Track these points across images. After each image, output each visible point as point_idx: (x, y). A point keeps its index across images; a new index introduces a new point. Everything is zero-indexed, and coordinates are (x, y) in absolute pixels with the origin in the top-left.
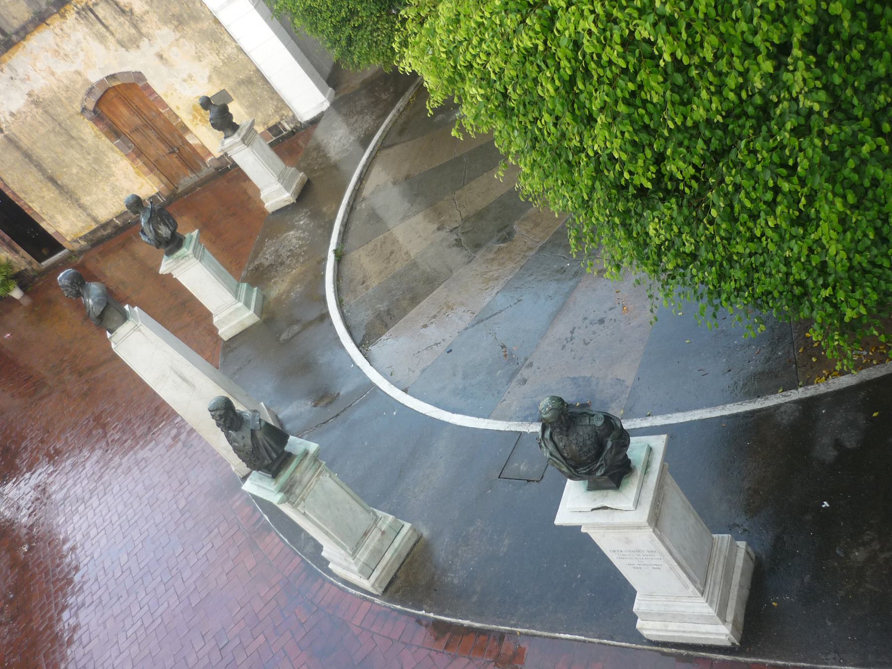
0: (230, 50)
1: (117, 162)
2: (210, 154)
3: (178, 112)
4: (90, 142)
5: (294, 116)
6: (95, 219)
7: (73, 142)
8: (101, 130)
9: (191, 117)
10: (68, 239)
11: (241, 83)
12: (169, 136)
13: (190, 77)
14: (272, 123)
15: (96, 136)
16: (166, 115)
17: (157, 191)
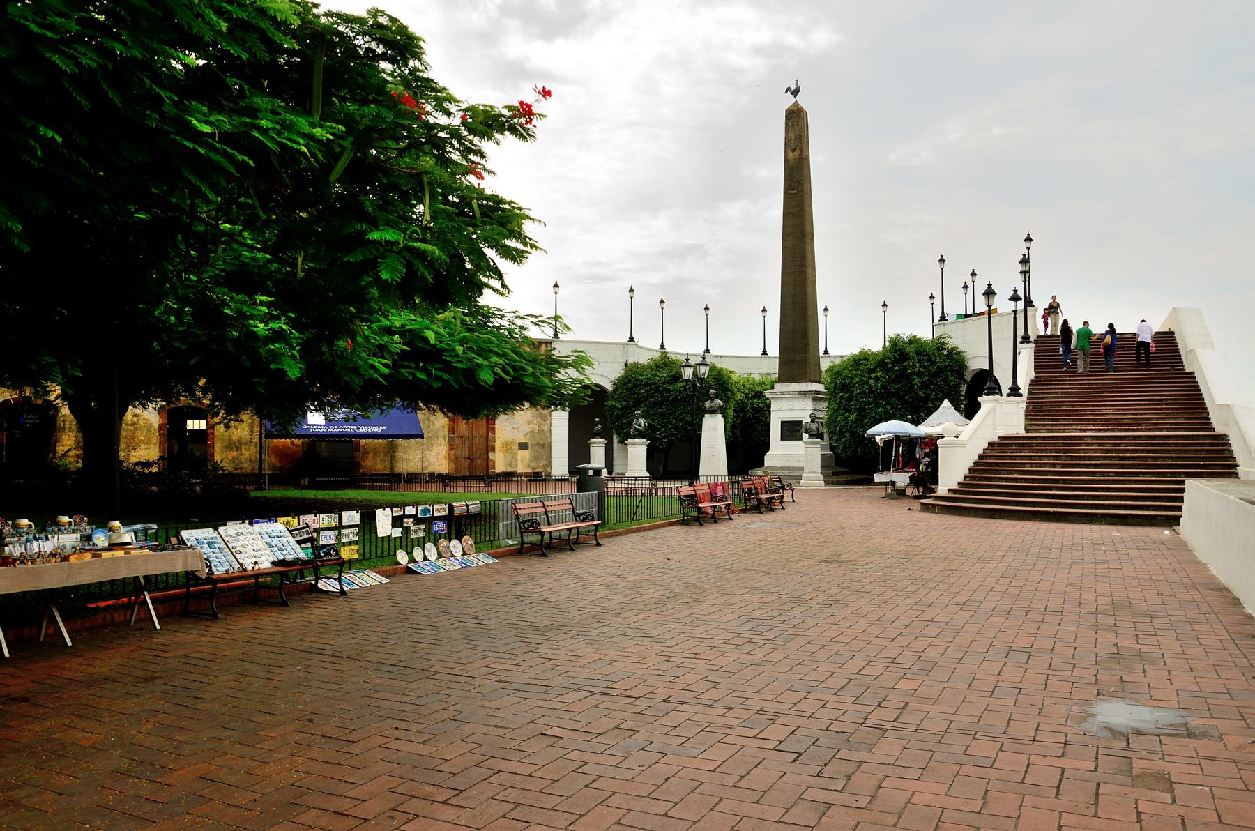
0: (546, 428)
1: (440, 445)
2: (494, 468)
3: (497, 440)
4: (436, 427)
5: (550, 473)
6: (392, 468)
7: (427, 422)
8: (449, 425)
9: (501, 446)
10: (361, 471)
11: (538, 444)
12: (474, 450)
13: (518, 428)
14: (536, 471)
15: (443, 427)
16: (491, 438)
17: (447, 472)
